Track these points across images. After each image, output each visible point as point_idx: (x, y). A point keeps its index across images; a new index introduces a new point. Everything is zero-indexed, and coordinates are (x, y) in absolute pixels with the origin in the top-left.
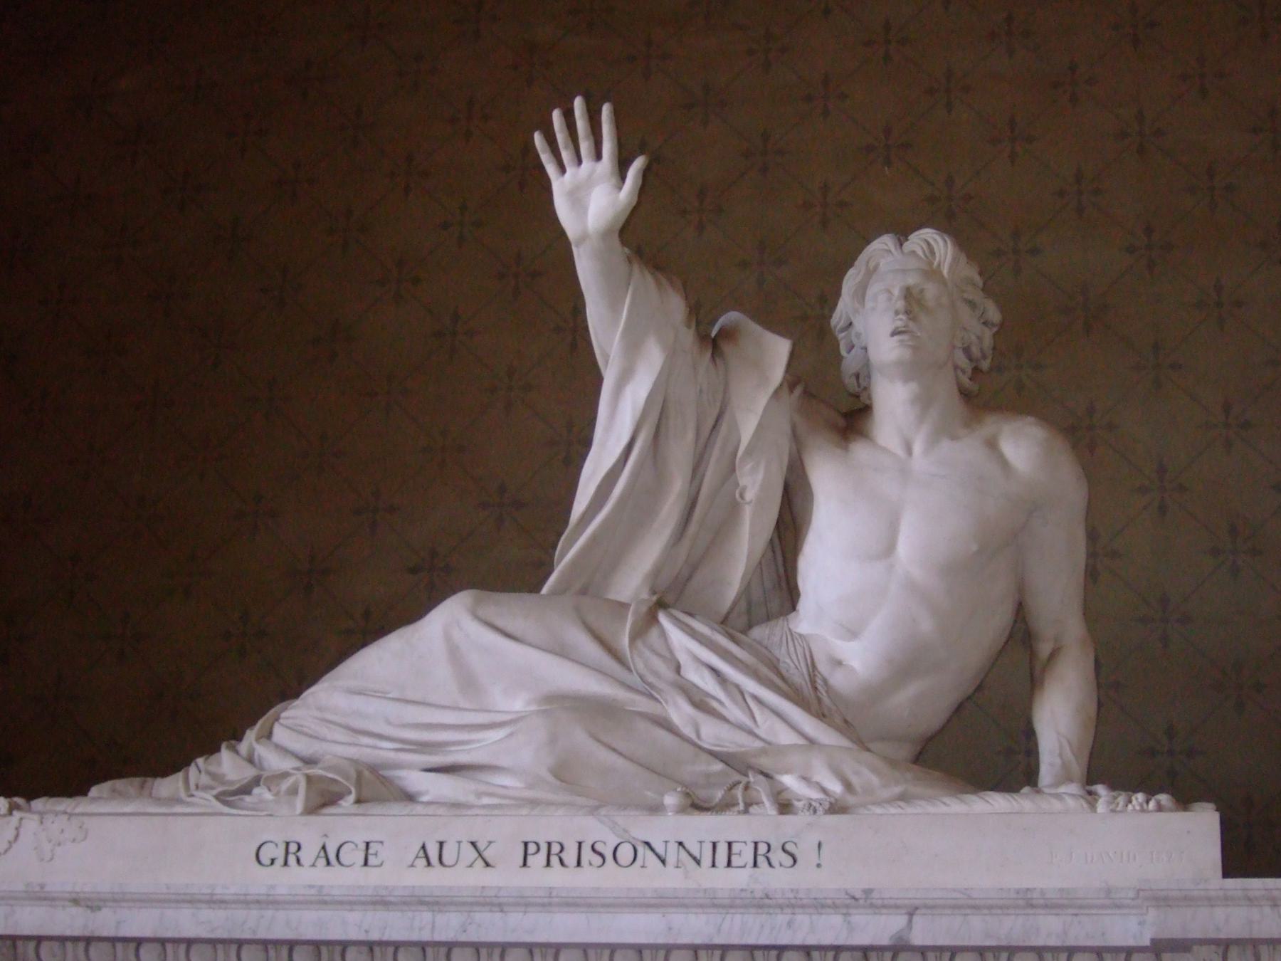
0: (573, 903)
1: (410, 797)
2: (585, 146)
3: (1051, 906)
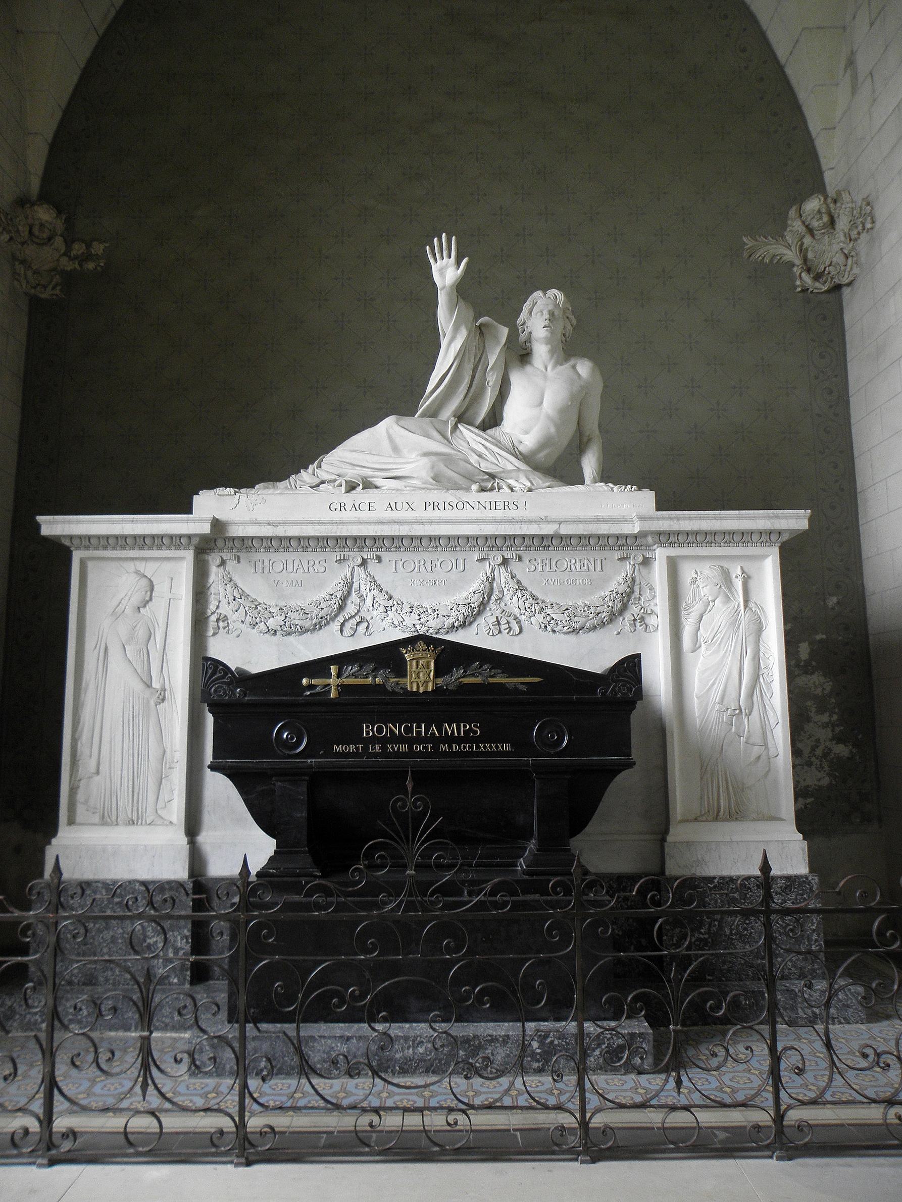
0: (447, 522)
1: (377, 487)
3: (605, 521)
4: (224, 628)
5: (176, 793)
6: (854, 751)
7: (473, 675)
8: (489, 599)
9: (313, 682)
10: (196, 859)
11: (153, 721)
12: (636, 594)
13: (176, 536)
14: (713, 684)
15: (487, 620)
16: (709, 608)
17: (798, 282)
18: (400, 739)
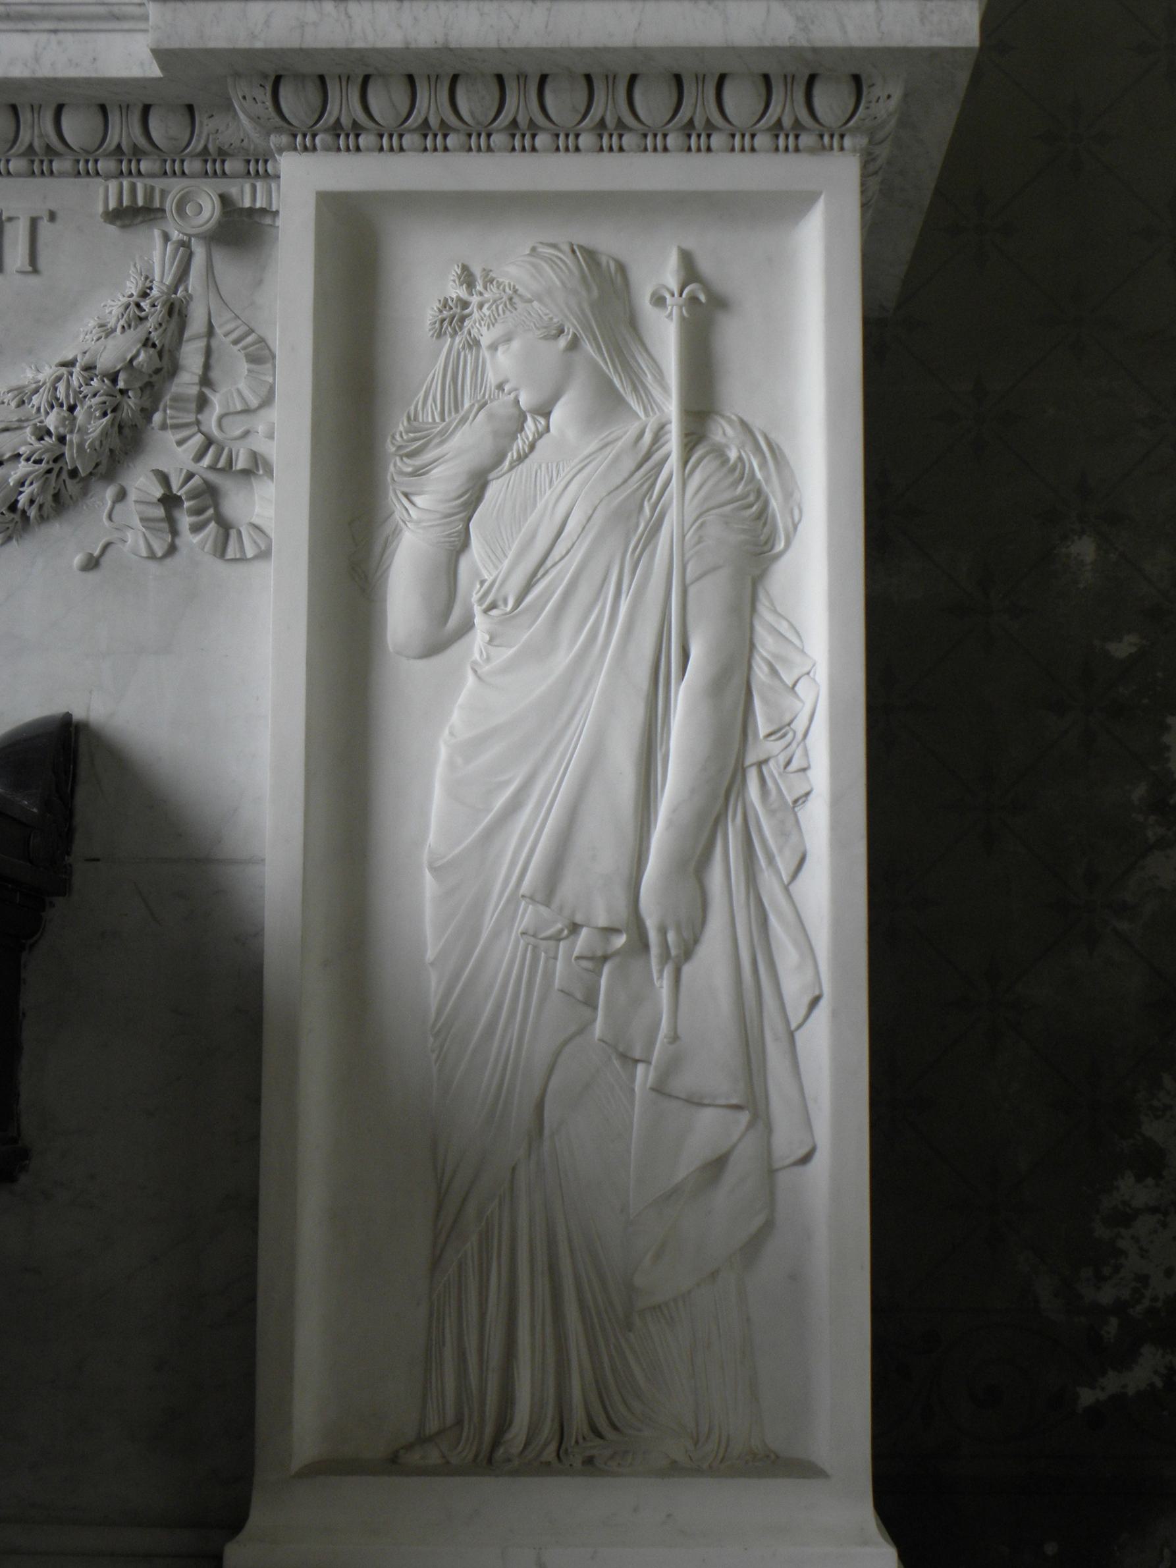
12: (186, 382)
14: (514, 806)
16: (520, 444)
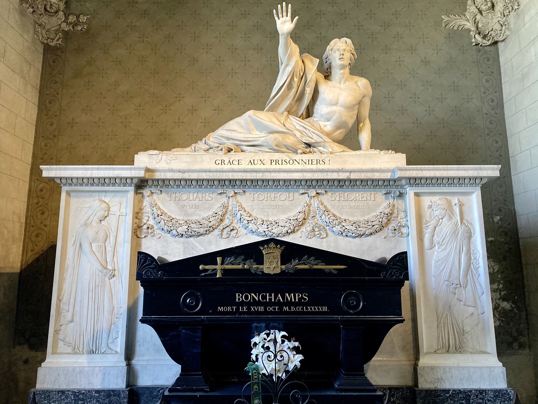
2: (284, 14)
4: (152, 233)
5: (120, 334)
6: (513, 306)
7: (304, 264)
8: (308, 216)
9: (207, 267)
10: (131, 373)
11: (107, 288)
13: (124, 178)
15: (307, 228)
17: (473, 40)
18: (258, 303)
